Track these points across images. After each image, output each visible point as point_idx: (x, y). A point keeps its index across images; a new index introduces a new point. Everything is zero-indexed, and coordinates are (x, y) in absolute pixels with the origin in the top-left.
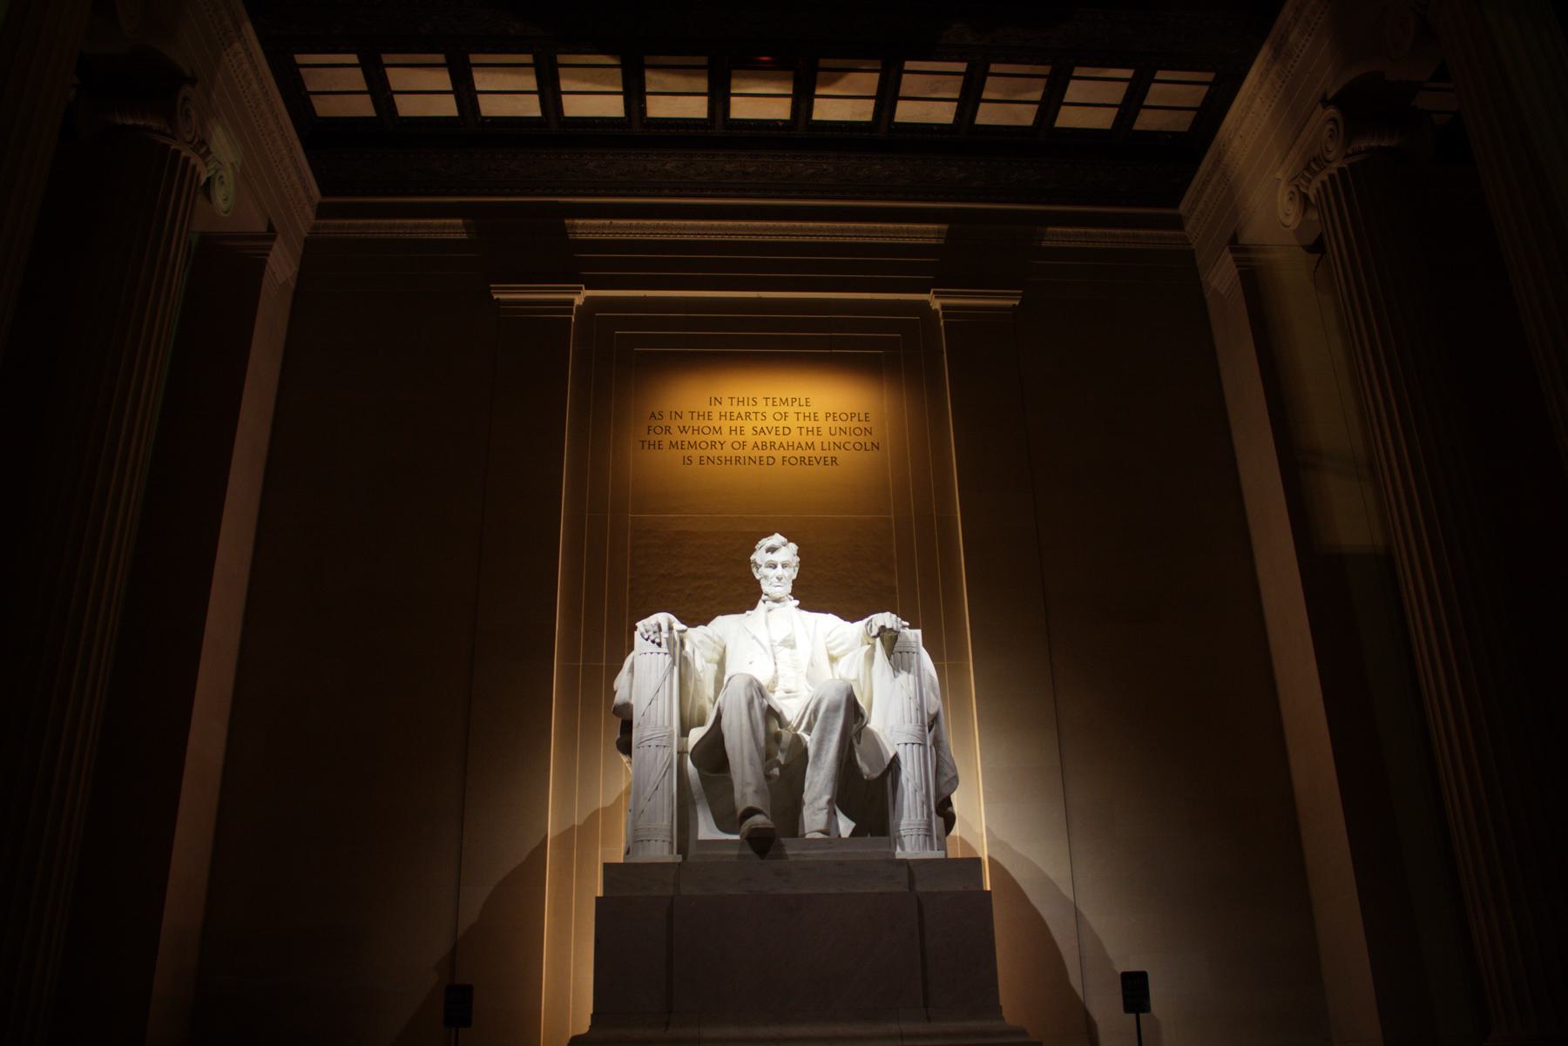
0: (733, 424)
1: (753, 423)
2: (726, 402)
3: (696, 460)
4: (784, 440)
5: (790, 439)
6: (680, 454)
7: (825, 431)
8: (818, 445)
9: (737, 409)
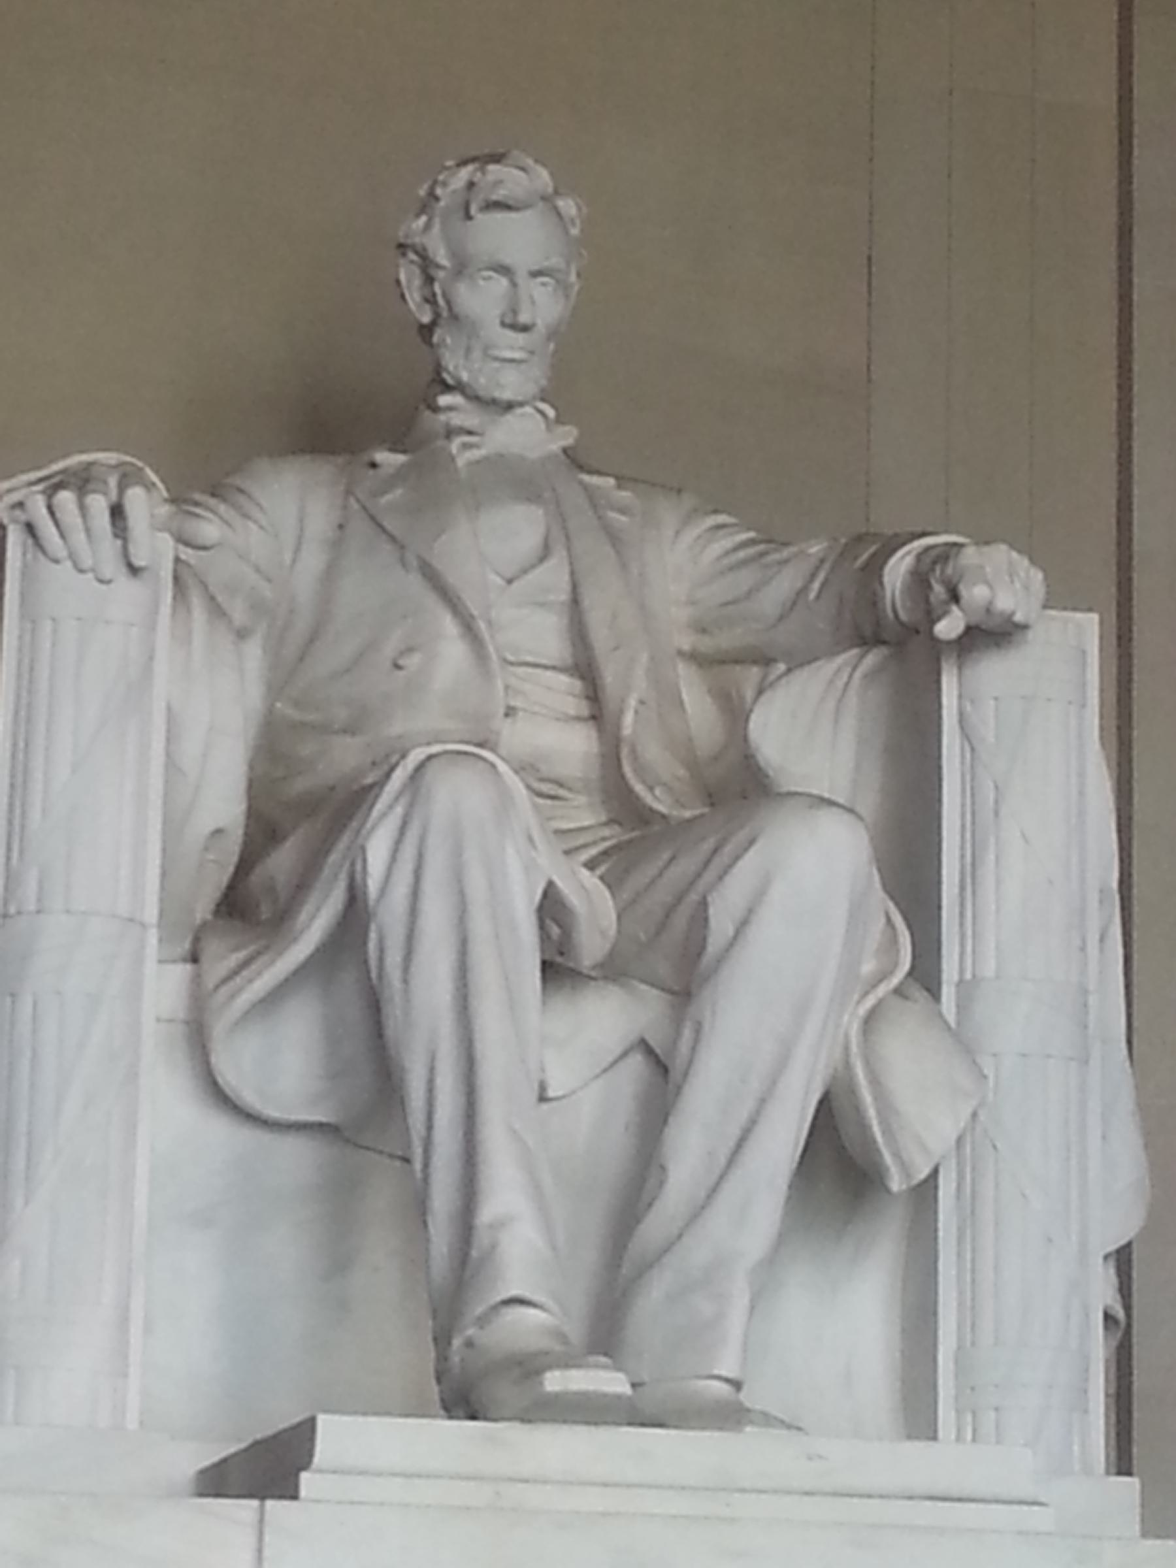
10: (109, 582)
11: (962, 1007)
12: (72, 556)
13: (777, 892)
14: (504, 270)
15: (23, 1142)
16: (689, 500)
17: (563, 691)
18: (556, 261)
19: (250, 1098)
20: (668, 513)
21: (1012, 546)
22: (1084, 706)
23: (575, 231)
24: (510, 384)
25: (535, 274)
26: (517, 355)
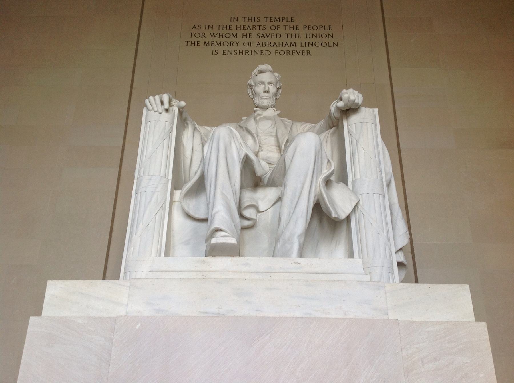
0: (245, 32)
1: (258, 32)
2: (241, 19)
3: (220, 52)
4: (277, 41)
5: (280, 40)
6: (210, 49)
7: (303, 36)
8: (298, 44)
9: (247, 24)
10: (161, 113)
11: (353, 186)
12: (153, 109)
13: (298, 150)
14: (263, 83)
15: (136, 223)
16: (303, 123)
17: (275, 149)
18: (271, 80)
19: (192, 213)
20: (298, 124)
21: (354, 89)
22: (376, 125)
23: (278, 78)
24: (266, 103)
25: (269, 83)
26: (267, 98)
